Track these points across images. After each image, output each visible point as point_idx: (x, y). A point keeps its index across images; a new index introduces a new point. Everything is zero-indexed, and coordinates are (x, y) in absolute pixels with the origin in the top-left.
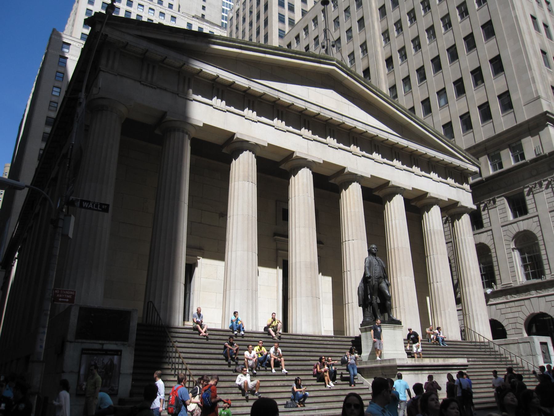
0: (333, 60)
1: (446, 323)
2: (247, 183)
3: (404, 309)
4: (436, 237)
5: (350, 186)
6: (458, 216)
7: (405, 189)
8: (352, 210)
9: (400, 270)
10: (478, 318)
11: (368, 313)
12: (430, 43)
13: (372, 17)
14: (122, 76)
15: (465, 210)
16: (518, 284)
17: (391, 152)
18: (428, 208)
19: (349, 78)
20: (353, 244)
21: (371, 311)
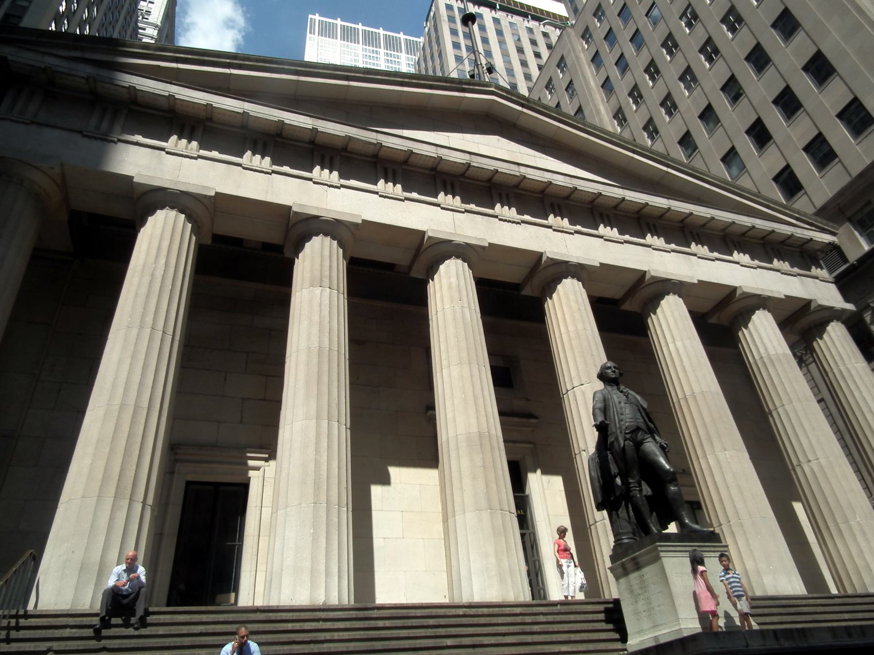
0: (490, 86)
1: (861, 552)
2: (318, 290)
3: (741, 525)
5: (559, 287)
6: (819, 328)
7: (681, 283)
8: (571, 328)
11: (625, 524)
12: (690, 94)
13: (593, 100)
14: (40, 125)
15: (830, 315)
17: (637, 223)
18: (744, 317)
20: (583, 393)
21: (633, 520)
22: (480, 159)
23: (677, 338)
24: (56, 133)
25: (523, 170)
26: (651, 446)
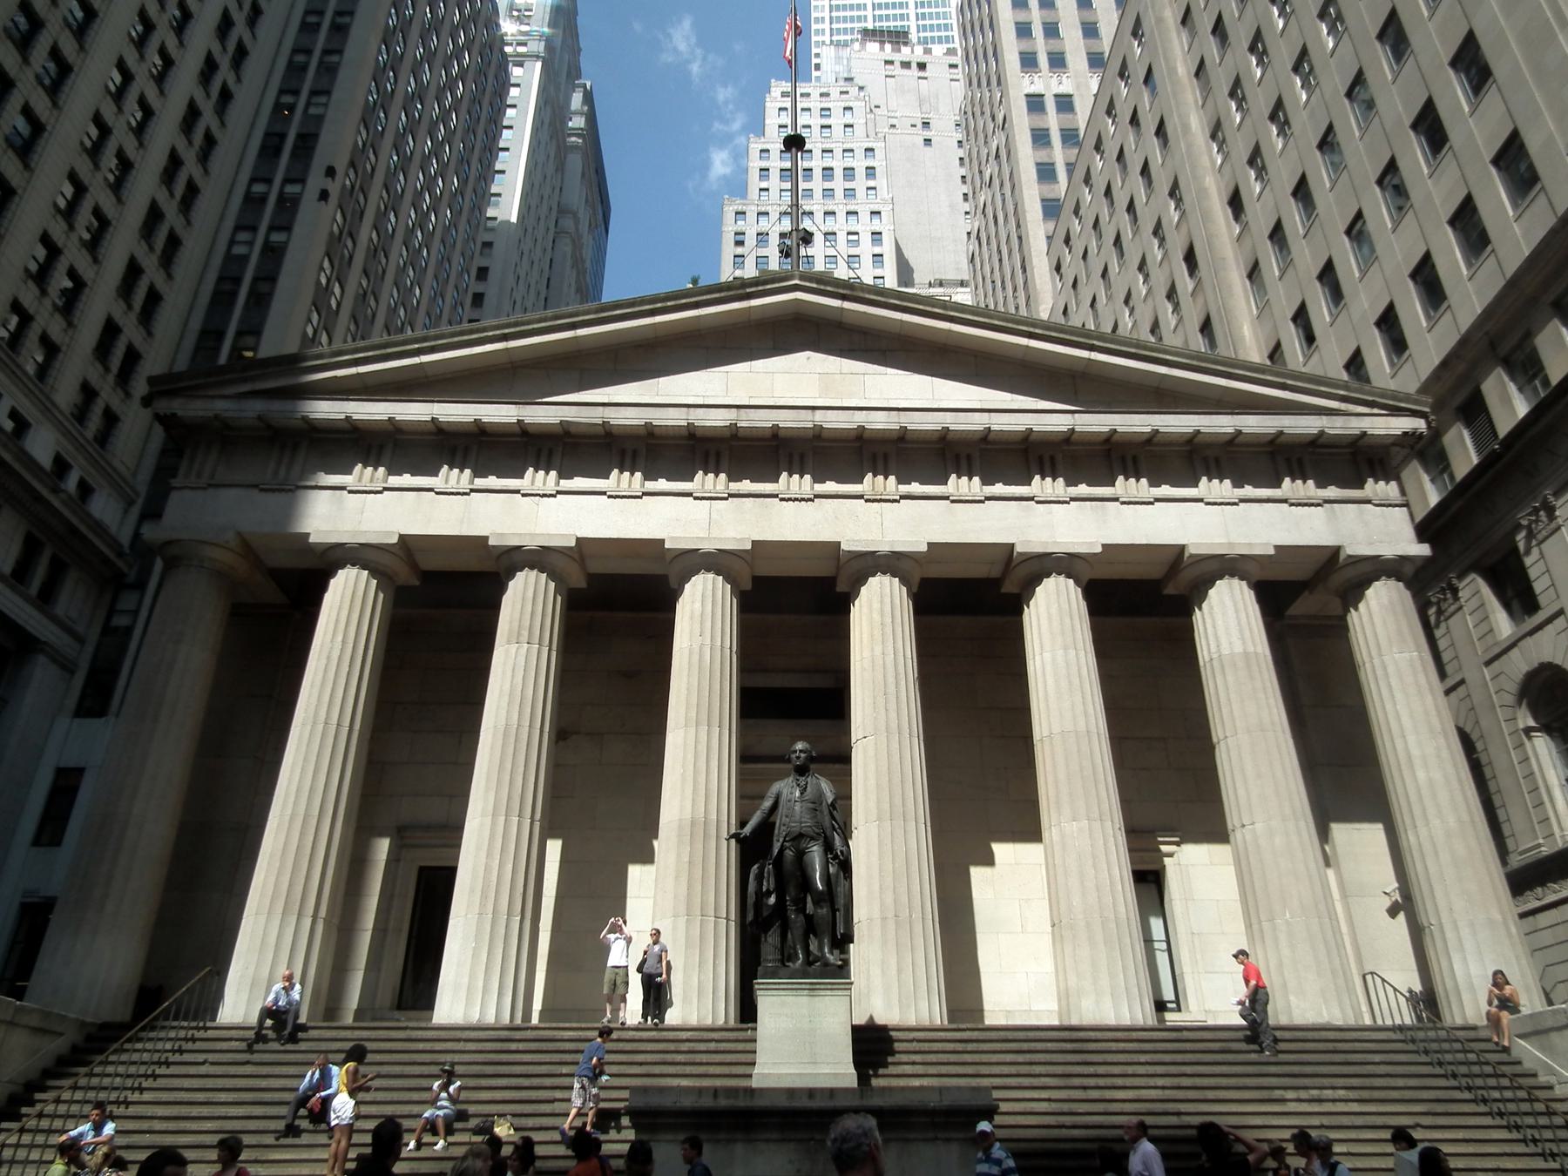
4: (1230, 678)
7: (1072, 556)
9: (1058, 802)
10: (1460, 940)
19: (847, 305)
22: (752, 413)
23: (1047, 647)
24: (233, 492)
25: (819, 417)
26: (815, 853)
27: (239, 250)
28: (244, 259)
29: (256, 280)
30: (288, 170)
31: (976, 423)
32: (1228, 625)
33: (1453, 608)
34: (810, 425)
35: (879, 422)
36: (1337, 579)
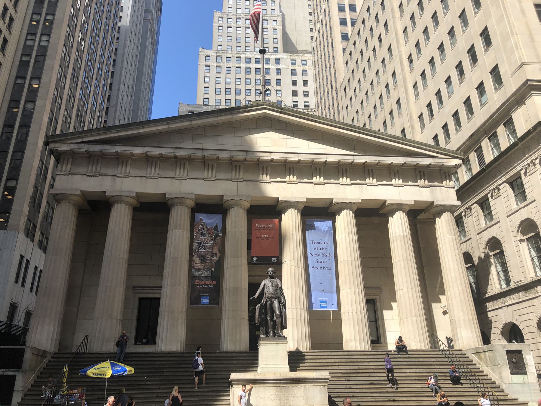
0: (263, 105)
16: (529, 280)
19: (281, 115)
24: (78, 176)
26: (276, 304)
27: (29, 43)
28: (32, 47)
29: (37, 56)
30: (47, 10)
31: (322, 158)
32: (398, 227)
33: (469, 215)
34: (270, 158)
35: (292, 158)
36: (432, 211)
